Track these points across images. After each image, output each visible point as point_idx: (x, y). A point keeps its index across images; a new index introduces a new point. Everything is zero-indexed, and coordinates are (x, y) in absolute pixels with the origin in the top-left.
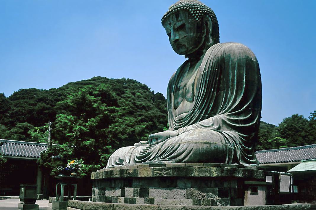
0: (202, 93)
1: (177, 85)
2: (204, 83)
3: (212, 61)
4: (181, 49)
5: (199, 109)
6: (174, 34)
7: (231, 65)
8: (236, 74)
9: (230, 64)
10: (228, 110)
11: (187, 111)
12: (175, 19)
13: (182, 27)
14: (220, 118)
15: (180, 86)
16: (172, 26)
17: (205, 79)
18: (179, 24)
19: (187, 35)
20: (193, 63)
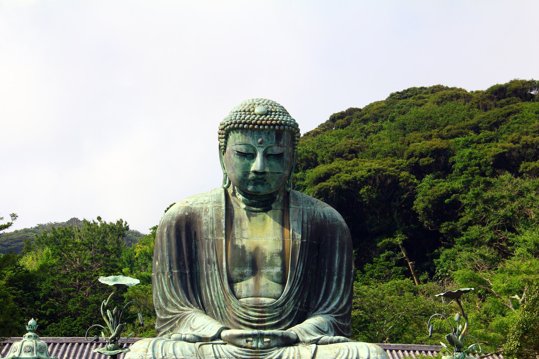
0: (299, 275)
1: (234, 240)
2: (303, 260)
3: (310, 226)
4: (259, 186)
5: (294, 299)
6: (263, 161)
7: (340, 244)
8: (345, 260)
9: (338, 242)
10: (335, 310)
11: (272, 296)
12: (275, 139)
13: (279, 157)
14: (331, 321)
15: (243, 247)
16: (262, 147)
17: (304, 253)
18: (276, 150)
19: (282, 171)
20: (254, 209)
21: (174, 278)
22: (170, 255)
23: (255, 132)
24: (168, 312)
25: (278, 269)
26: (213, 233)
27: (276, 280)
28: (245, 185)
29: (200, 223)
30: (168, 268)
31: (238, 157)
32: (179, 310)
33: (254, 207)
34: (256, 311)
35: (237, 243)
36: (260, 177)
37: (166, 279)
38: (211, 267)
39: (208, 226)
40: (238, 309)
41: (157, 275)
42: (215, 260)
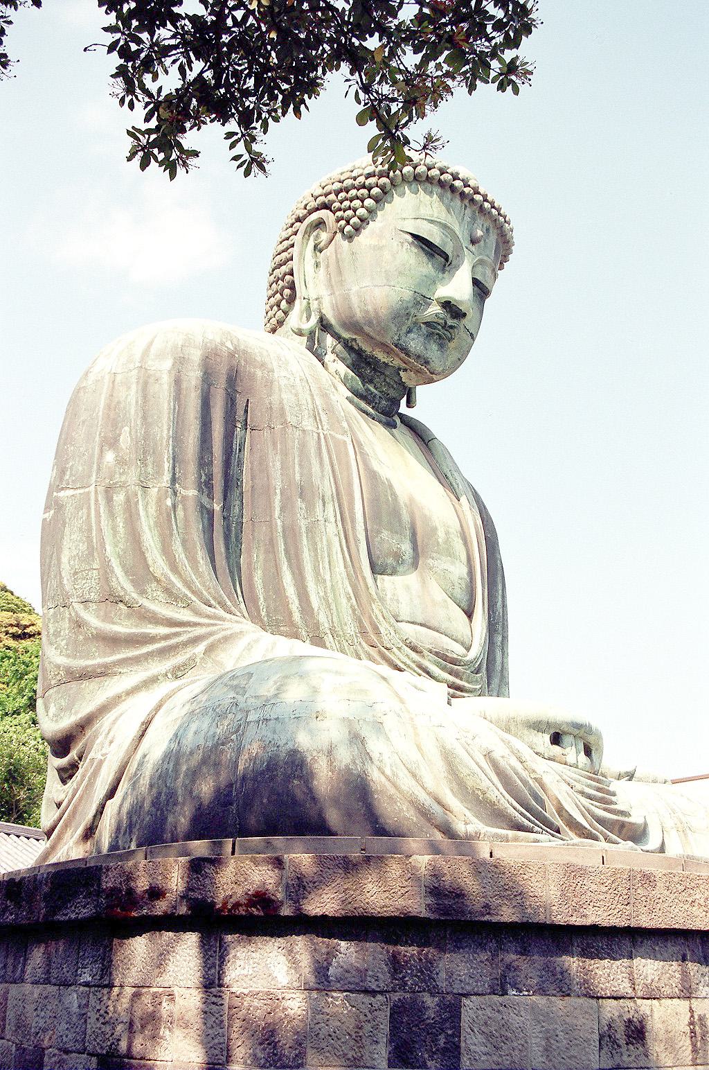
4: (434, 347)
21: (180, 512)
22: (177, 439)
23: (468, 211)
24: (154, 613)
25: (460, 570)
26: (316, 417)
27: (459, 596)
28: (404, 329)
29: (269, 384)
30: (167, 477)
31: (415, 250)
32: (197, 613)
33: (369, 403)
34: (443, 669)
35: (375, 469)
36: (450, 322)
37: (152, 510)
38: (310, 508)
39: (296, 395)
40: (399, 649)
41: (109, 491)
42: (327, 488)
